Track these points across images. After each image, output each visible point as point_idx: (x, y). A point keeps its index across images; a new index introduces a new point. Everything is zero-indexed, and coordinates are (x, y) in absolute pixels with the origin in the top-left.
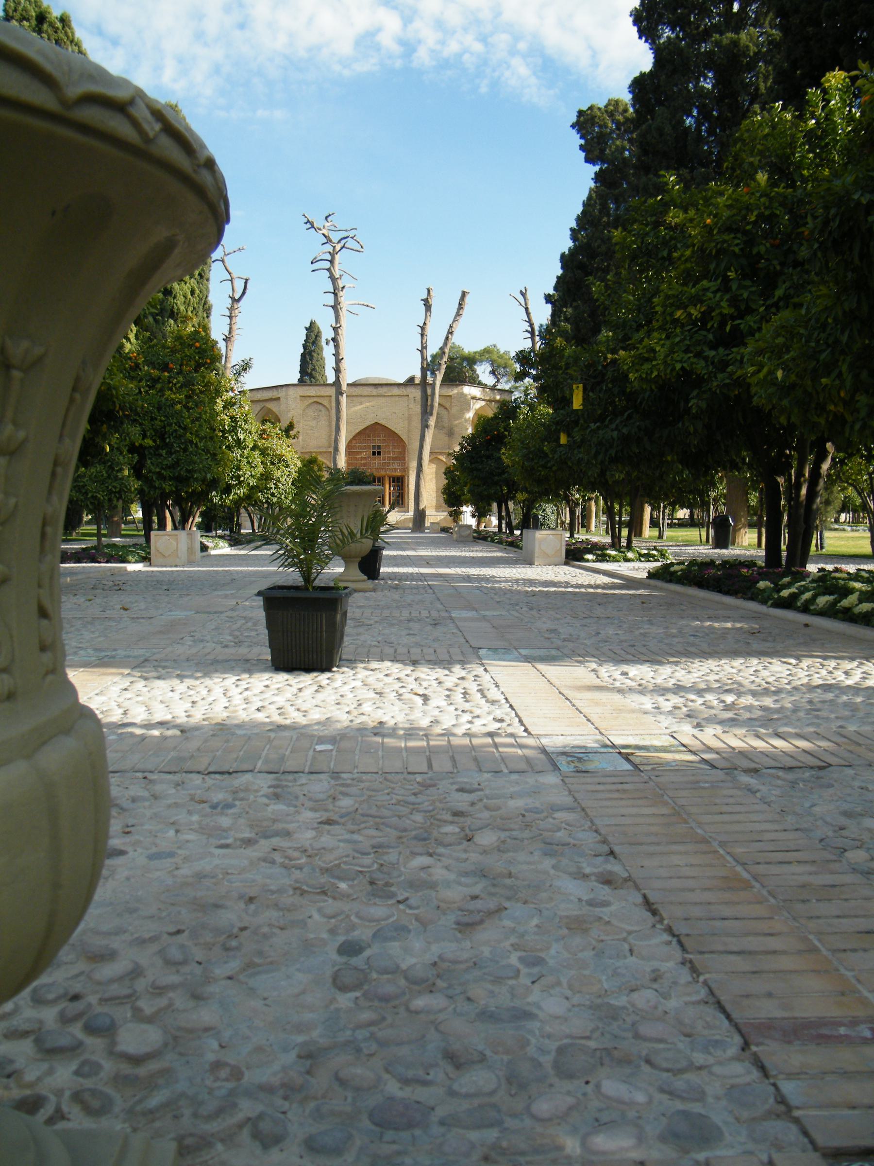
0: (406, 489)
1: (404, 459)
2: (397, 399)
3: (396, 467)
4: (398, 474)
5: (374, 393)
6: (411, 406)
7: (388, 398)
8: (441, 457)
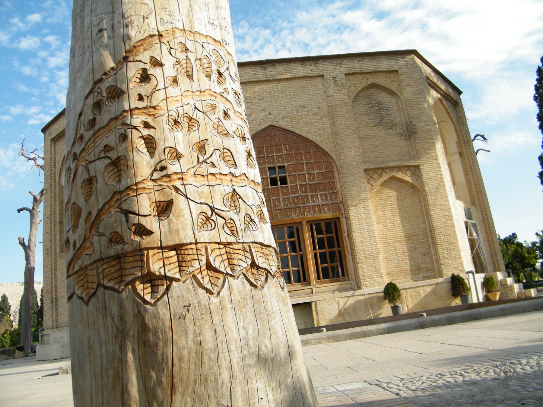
0: (347, 243)
1: (332, 185)
2: (303, 83)
3: (320, 202)
4: (328, 215)
5: (261, 77)
6: (331, 92)
7: (286, 84)
8: (399, 175)
